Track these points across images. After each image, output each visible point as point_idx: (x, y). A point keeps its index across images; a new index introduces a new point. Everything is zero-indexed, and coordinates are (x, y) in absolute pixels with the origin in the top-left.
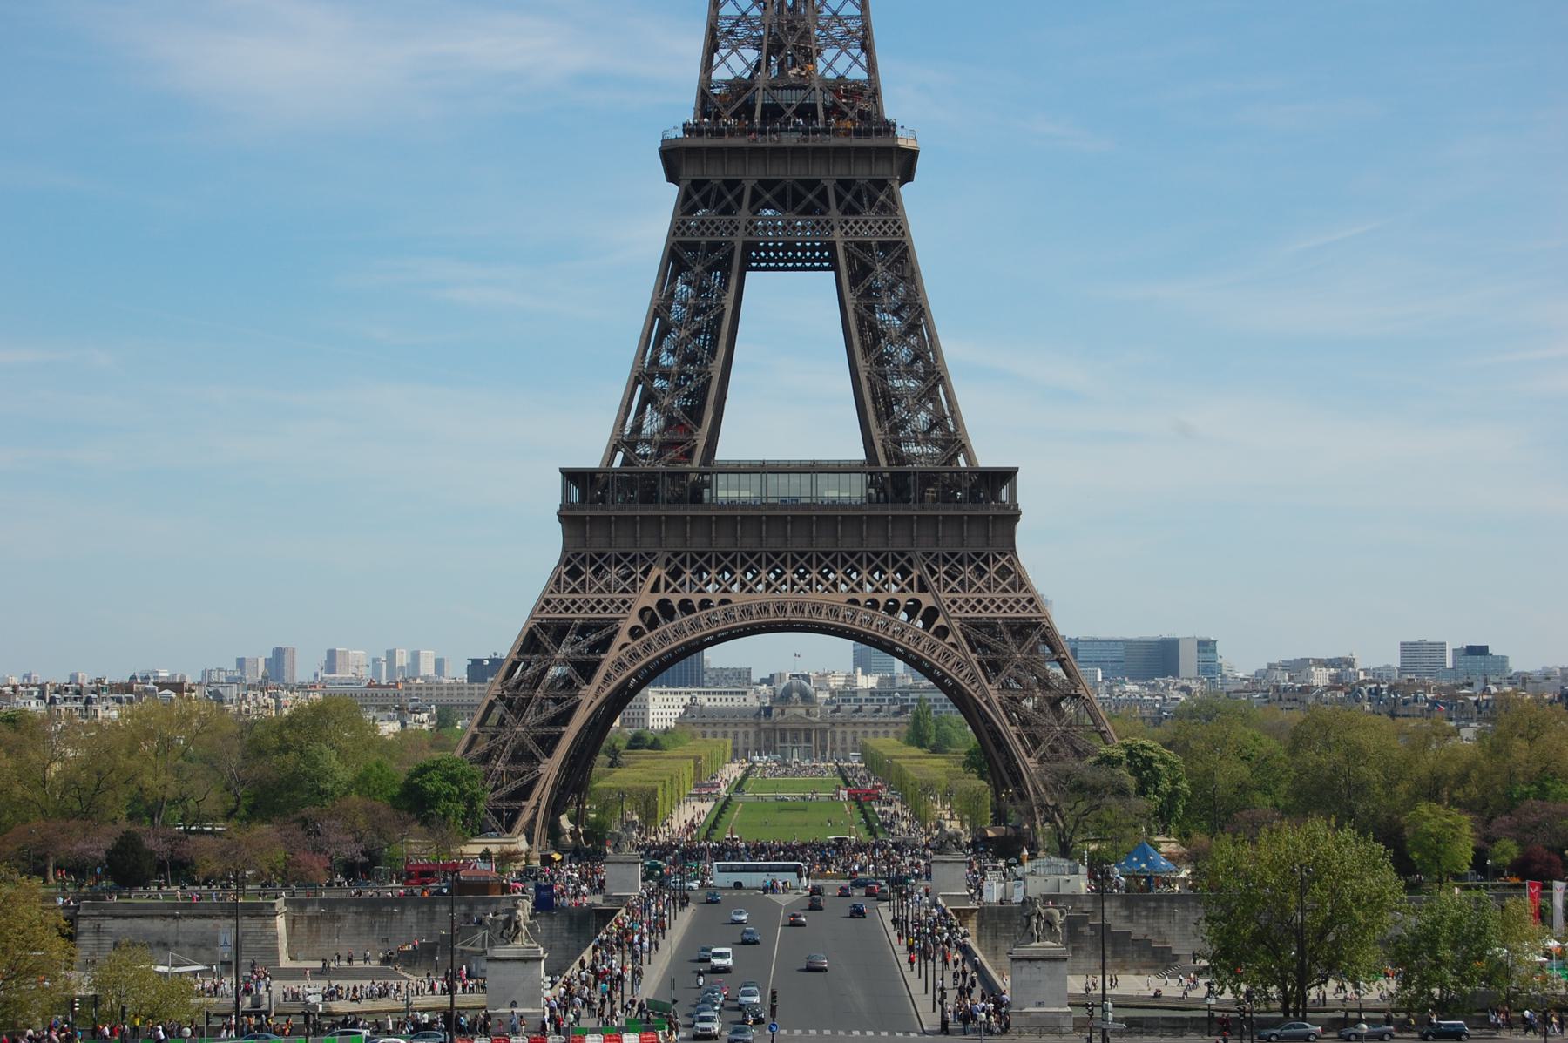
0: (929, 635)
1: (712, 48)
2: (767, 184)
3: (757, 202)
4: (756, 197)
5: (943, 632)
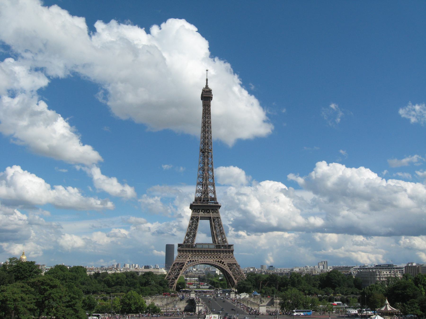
0: (223, 265)
5: (225, 265)
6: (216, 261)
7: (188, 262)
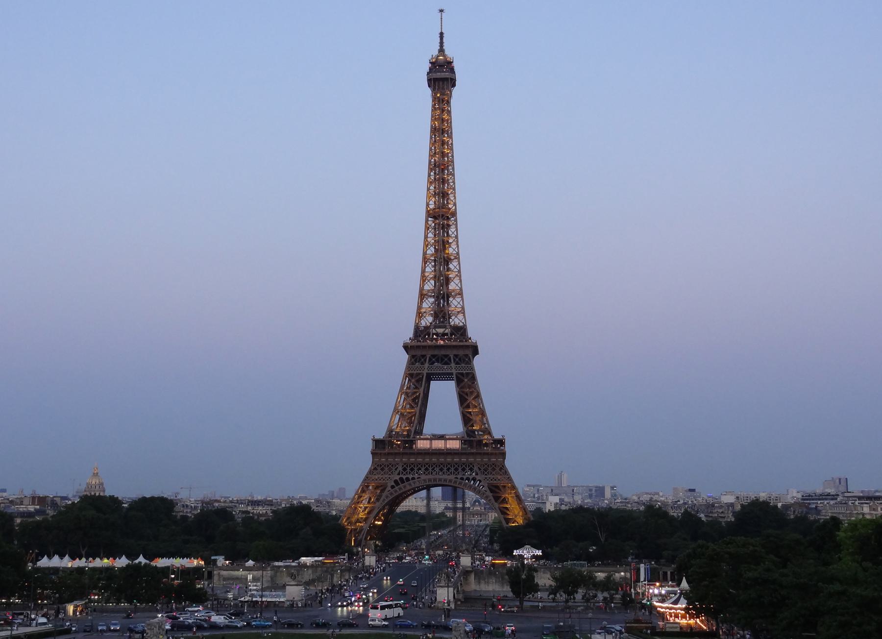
1: (420, 315)
2: (434, 356)
4: (430, 360)
6: (462, 479)
7: (396, 481)
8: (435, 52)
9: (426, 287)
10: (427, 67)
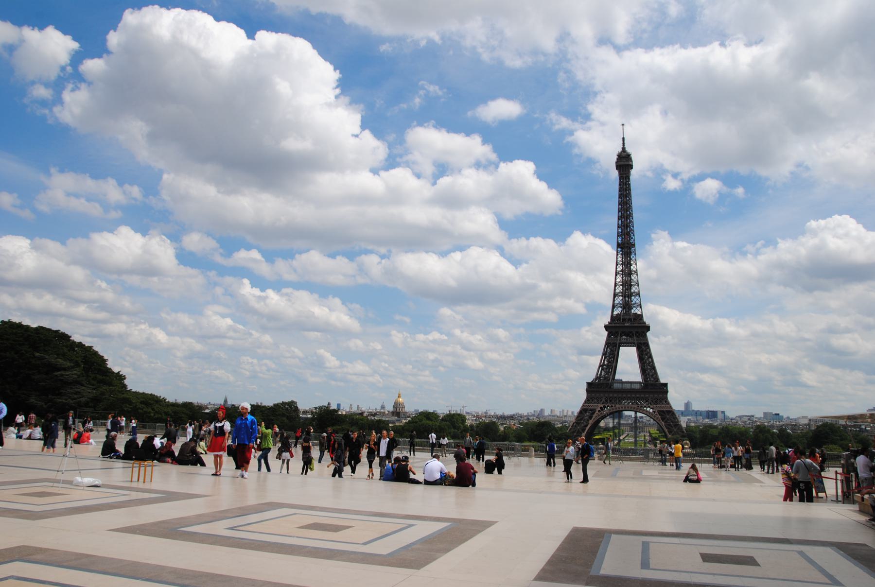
1: (614, 307)
3: (621, 336)
8: (620, 150)
9: (617, 291)
10: (615, 158)
